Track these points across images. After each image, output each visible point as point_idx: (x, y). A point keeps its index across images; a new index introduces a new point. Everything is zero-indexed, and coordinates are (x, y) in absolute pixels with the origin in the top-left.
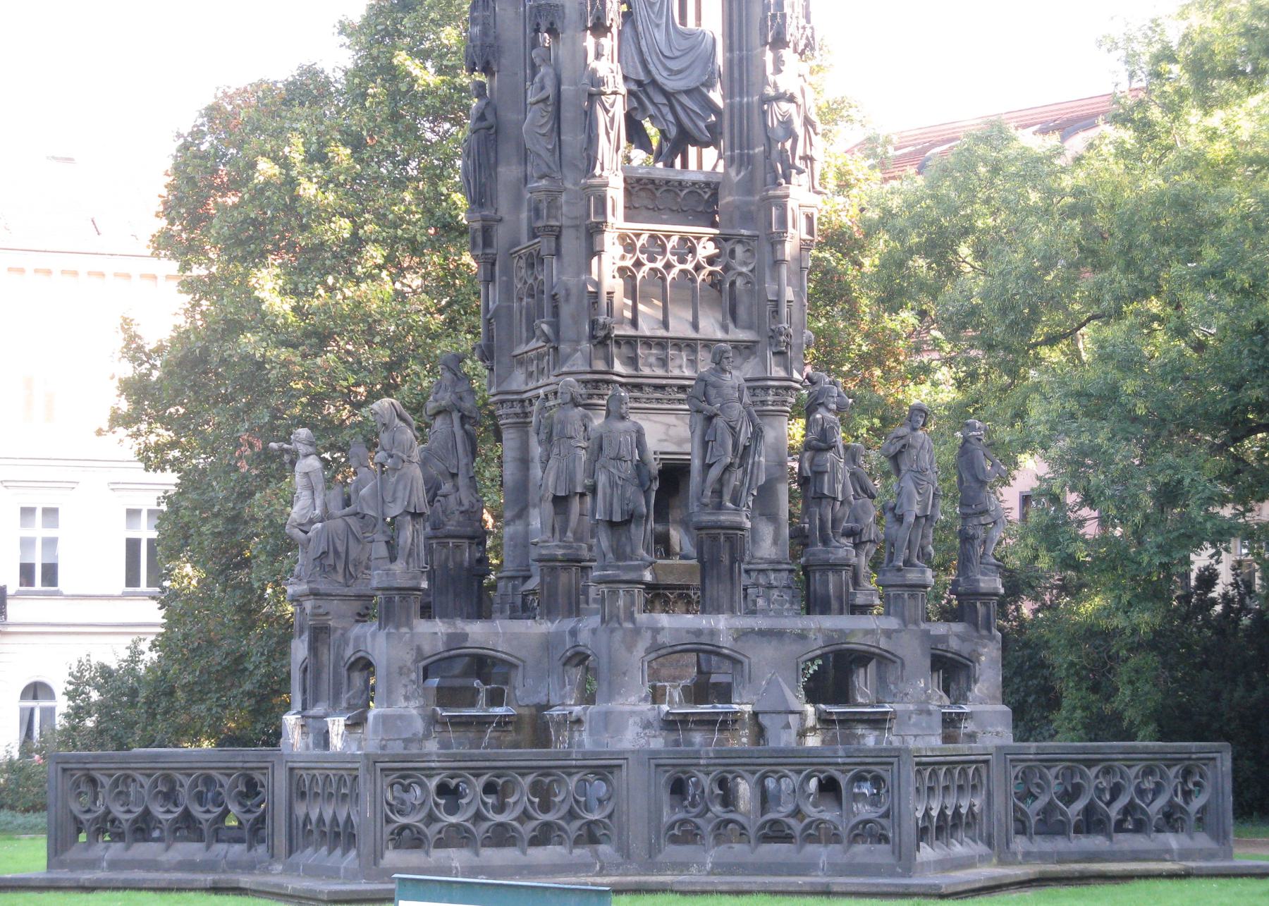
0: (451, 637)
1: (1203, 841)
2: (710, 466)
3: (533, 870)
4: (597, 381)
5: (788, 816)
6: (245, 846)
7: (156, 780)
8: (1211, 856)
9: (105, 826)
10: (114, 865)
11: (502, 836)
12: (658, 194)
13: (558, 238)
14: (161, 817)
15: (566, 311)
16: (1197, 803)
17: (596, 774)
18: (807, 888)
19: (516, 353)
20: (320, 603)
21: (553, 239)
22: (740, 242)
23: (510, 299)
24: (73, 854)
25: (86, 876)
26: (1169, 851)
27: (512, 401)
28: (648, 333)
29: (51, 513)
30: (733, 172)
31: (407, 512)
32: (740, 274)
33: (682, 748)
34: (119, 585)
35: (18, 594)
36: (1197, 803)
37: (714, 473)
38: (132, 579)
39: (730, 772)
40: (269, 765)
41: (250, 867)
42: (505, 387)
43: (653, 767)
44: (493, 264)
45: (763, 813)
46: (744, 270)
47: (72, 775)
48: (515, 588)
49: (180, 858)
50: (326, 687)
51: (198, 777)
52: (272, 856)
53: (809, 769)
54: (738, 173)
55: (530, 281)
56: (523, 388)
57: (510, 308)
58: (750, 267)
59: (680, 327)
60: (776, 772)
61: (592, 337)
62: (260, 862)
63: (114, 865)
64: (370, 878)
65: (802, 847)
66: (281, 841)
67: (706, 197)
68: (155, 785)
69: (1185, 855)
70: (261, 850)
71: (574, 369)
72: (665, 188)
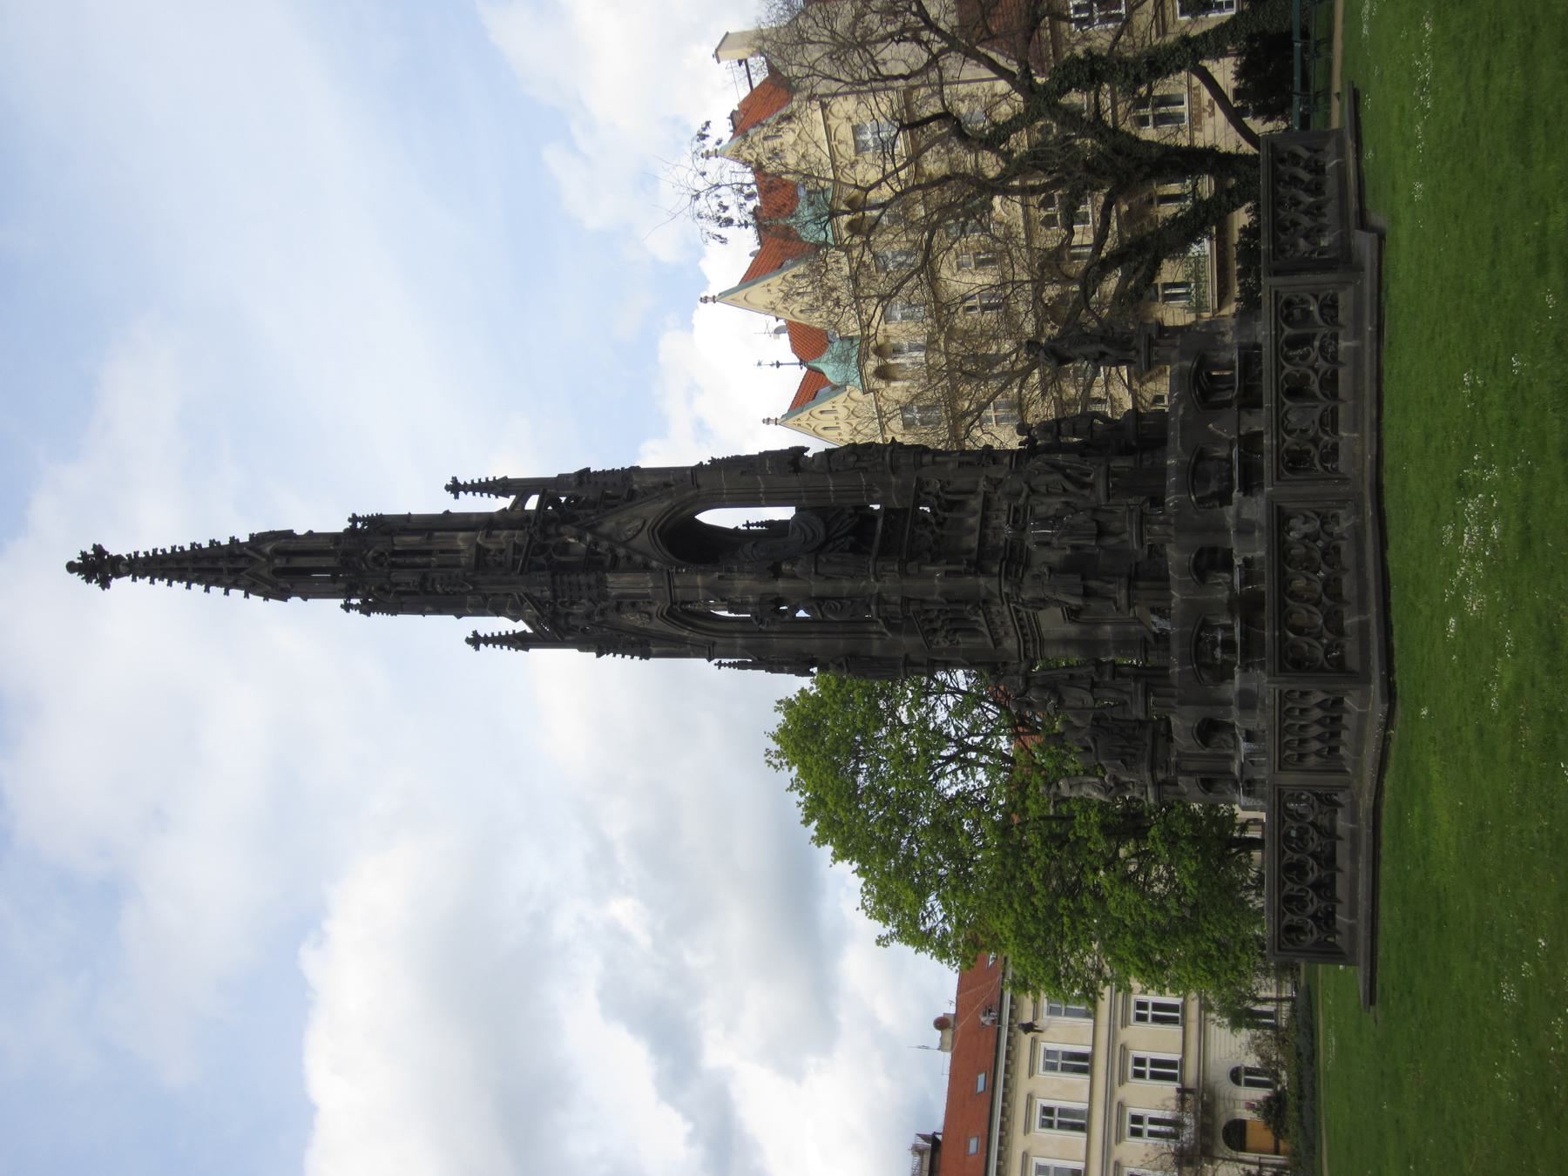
1: (1331, 146)
2: (1065, 490)
3: (1360, 564)
6: (1338, 843)
9: (1326, 920)
10: (1353, 913)
11: (1332, 587)
24: (1345, 948)
25: (1363, 932)
26: (1338, 164)
29: (1140, 1062)
31: (1091, 691)
32: (942, 488)
34: (1177, 1029)
35: (1182, 1082)
37: (1069, 486)
38: (1173, 1021)
41: (1354, 804)
45: (1313, 397)
59: (973, 521)
61: (975, 574)
63: (1353, 913)
64: (1368, 681)
65: (1341, 326)
66: (1335, 779)
68: (1291, 880)
69: (1341, 153)
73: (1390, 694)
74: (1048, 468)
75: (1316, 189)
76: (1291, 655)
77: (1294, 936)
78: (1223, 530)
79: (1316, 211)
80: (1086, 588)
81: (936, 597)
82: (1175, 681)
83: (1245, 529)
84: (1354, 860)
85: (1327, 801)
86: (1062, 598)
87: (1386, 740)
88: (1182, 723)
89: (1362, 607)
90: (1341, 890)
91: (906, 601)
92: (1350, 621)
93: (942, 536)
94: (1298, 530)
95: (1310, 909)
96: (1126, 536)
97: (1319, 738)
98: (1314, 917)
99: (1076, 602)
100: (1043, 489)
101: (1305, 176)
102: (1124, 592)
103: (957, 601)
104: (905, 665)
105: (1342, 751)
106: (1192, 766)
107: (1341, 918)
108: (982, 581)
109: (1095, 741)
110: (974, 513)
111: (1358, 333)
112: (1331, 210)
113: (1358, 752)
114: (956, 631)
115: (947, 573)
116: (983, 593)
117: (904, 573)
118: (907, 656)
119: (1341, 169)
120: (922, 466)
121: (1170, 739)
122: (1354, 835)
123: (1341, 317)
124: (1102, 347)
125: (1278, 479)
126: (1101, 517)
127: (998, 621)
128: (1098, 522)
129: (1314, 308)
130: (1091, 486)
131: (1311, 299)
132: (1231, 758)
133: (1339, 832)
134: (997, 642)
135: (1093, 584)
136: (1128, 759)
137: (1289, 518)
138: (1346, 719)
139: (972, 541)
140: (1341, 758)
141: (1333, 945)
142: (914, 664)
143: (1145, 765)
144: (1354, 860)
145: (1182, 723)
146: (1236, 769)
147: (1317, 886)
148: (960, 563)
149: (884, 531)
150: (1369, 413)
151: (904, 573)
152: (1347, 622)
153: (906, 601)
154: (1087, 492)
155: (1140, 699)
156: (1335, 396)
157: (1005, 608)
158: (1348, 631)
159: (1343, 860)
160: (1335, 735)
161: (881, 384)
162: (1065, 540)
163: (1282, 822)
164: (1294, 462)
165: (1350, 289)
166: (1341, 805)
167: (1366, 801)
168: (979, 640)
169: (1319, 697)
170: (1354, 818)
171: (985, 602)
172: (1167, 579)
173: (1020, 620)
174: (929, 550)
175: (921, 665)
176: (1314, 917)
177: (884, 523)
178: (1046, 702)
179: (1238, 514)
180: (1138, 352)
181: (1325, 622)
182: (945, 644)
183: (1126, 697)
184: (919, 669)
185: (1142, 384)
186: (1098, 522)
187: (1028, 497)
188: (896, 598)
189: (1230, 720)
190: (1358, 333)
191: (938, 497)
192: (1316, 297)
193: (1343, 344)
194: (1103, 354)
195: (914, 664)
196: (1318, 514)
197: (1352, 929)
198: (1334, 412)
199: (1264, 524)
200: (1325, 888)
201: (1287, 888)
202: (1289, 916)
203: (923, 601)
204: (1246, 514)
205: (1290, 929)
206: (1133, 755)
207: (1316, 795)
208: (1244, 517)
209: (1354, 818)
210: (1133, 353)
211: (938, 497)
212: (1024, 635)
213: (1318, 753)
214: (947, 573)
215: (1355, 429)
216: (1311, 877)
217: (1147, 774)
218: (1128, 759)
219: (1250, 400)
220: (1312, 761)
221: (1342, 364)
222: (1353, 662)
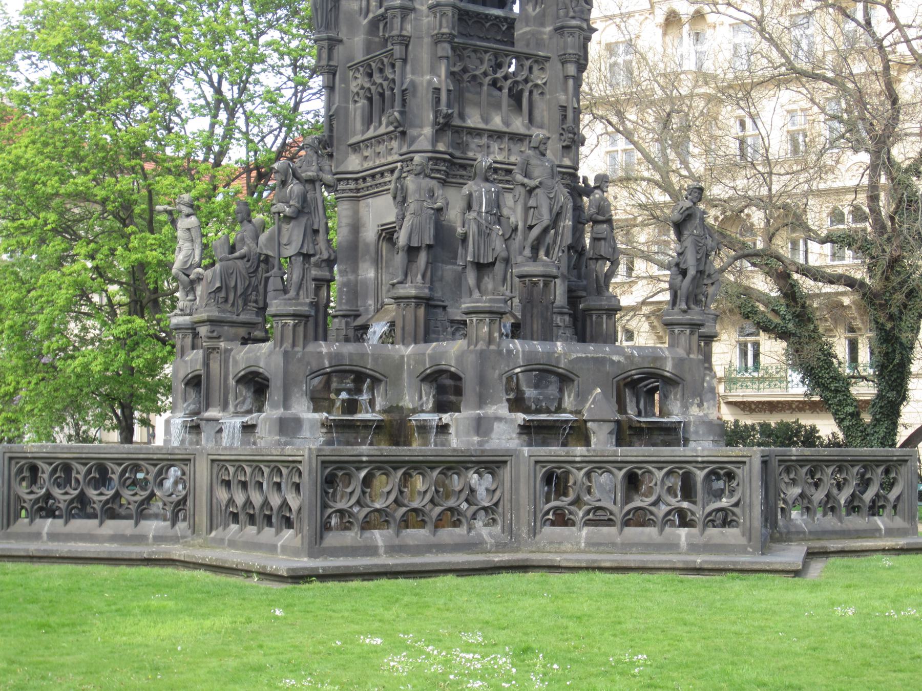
0: (330, 356)
1: (899, 522)
2: (531, 228)
3: (441, 548)
4: (437, 159)
5: (570, 504)
6: (132, 522)
7: (91, 468)
8: (902, 533)
10: (53, 536)
11: (415, 518)
12: (470, 23)
13: (407, 46)
14: (96, 498)
15: (412, 102)
16: (893, 495)
17: (486, 468)
18: (680, 565)
19: (353, 140)
20: (214, 328)
21: (404, 47)
22: (536, 62)
23: (347, 102)
24: (14, 528)
25: (33, 547)
26: (879, 530)
27: (348, 179)
28: (472, 125)
30: (530, 8)
31: (299, 254)
32: (536, 86)
33: (439, 448)
36: (893, 495)
37: (535, 232)
39: (640, 468)
40: (191, 457)
41: (175, 539)
42: (341, 169)
43: (532, 463)
44: (334, 75)
45: (627, 499)
46: (539, 82)
47: (17, 463)
48: (347, 324)
49: (111, 532)
50: (217, 394)
51: (24, 464)
52: (194, 532)
53: (590, 466)
54: (534, 10)
55: (367, 85)
56: (359, 168)
57: (347, 109)
58: (544, 81)
60: (600, 468)
61: (436, 123)
62: (184, 537)
63: (53, 536)
64: (311, 555)
66: (203, 519)
67: (504, 28)
68: (89, 472)
69: (890, 533)
70: (181, 526)
71: (419, 148)
72: (475, 19)
73: (297, 578)
74: (556, 209)
75: (853, 507)
76: (340, 473)
77: (26, 474)
78: (482, 401)
79: (829, 505)
80: (418, 249)
81: (409, 77)
82: (311, 347)
83: (481, 426)
84: (114, 538)
85: (179, 509)
86: (407, 224)
87: (248, 573)
88: (264, 356)
89: (392, 549)
90: (79, 525)
91: (405, 42)
92: (378, 537)
93: (481, 84)
94: (481, 483)
95: (57, 492)
96: (476, 295)
97: (248, 503)
98: (48, 496)
99: (402, 238)
100: (532, 203)
101: (869, 496)
102: (413, 292)
103: (404, 102)
104: (329, 39)
105: (234, 527)
106: (215, 366)
107: (47, 525)
108: (428, 131)
109: (242, 257)
110: (507, 123)
111: (693, 548)
112: (830, 522)
113: (233, 544)
114: (370, 100)
115: (437, 90)
116: (413, 132)
117: (437, 40)
118: (341, 41)
119: (873, 533)
120: (564, 63)
121: (245, 341)
122: (140, 539)
123: (713, 531)
124: (692, 272)
125: (537, 462)
126: (499, 268)
127: (381, 148)
128: (493, 264)
129: (724, 502)
130: (535, 257)
131: (734, 500)
132: (225, 407)
133: (144, 523)
134: (355, 147)
135: (423, 258)
136: (223, 294)
137: (493, 474)
138: (269, 532)
139: (474, 120)
140: (226, 526)
141: (18, 516)
142: (330, 50)
143: (215, 313)
144: (114, 538)
145: (264, 356)
146: (212, 413)
147: (82, 499)
148: (449, 106)
149: (487, 17)
150: (607, 559)
151: (437, 40)
152: (377, 533)
153: (405, 42)
154: (527, 252)
155: (291, 309)
156: (627, 523)
157: (396, 157)
158: (367, 534)
159: (112, 526)
160: (252, 519)
161: (660, 17)
162: (473, 229)
163: (154, 462)
164: (555, 480)
165: (743, 541)
166: (173, 525)
167: (178, 551)
168: (359, 126)
169: (294, 502)
170: (159, 539)
171: (403, 133)
172: (427, 340)
173: (382, 174)
174: (465, 70)
175: (330, 58)
176: (48, 496)
177: (497, 17)
178: (287, 202)
179: (499, 419)
180: (685, 312)
181: (377, 510)
182: (354, 87)
183: (292, 293)
184: (325, 55)
185: (648, 317)
186: (493, 264)
187: (523, 185)
188: (409, 29)
189: (267, 407)
190: (693, 548)
191: (526, 81)
192: (736, 505)
193: (683, 532)
194: (684, 273)
195: (330, 50)
196: (496, 504)
197: (37, 536)
198: (610, 522)
199: (487, 447)
200: (81, 507)
201: (79, 467)
202: (48, 469)
203: (405, 61)
204: (498, 427)
205: (34, 469)
206: (226, 300)
207: (185, 499)
208: (496, 425)
209: (159, 539)
210: (684, 307)
211: (526, 81)
212: (364, 179)
213: (231, 501)
214: (437, 90)
215: (588, 544)
216: (92, 493)
217: (204, 316)
218: (223, 294)
219: (625, 433)
220: (222, 495)
221: (662, 530)
222: (332, 539)
